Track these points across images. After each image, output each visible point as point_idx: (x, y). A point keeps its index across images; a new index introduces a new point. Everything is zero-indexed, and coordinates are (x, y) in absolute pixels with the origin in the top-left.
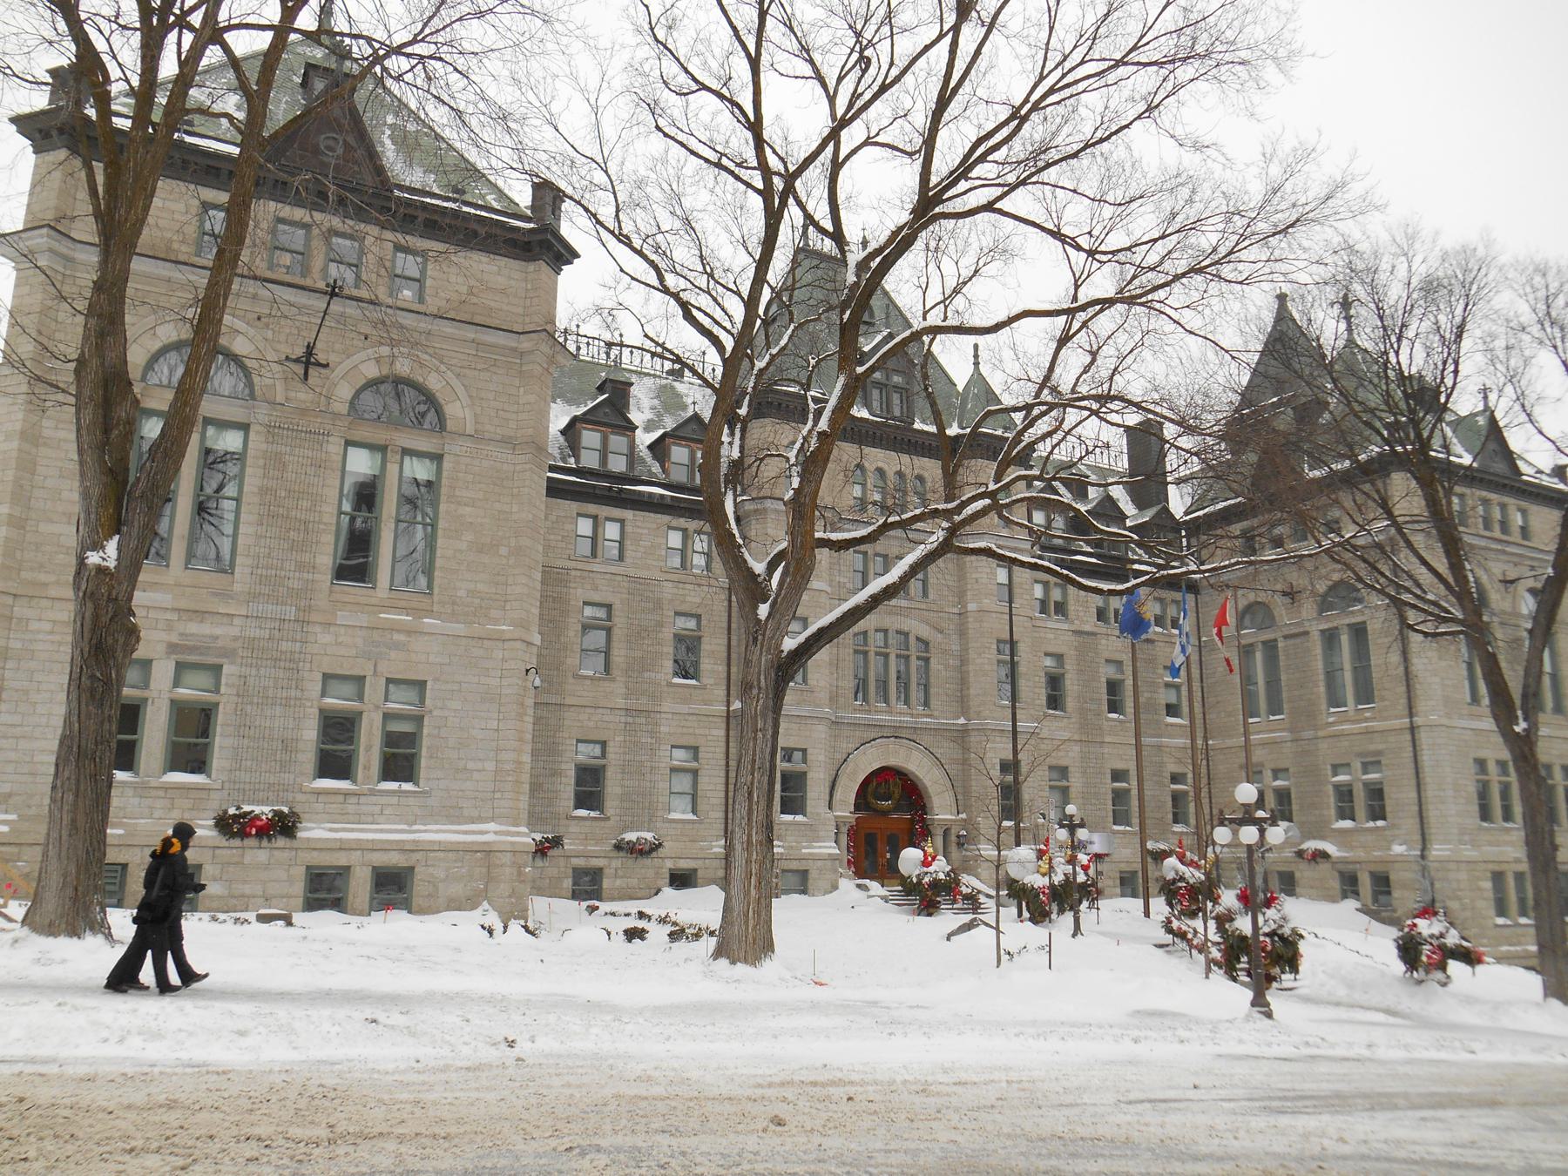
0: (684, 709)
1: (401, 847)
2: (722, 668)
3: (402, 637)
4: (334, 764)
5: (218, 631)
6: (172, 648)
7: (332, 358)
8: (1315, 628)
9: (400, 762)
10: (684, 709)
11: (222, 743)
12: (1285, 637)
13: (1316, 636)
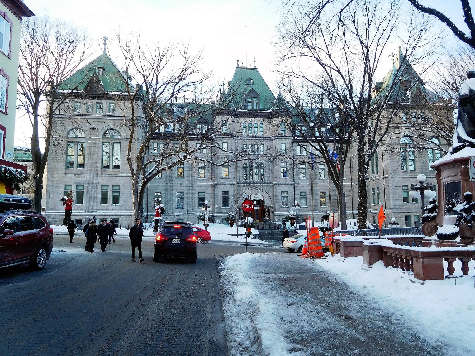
0: (201, 184)
1: (116, 215)
6: (75, 183)
7: (98, 128)
9: (116, 200)
10: (201, 184)
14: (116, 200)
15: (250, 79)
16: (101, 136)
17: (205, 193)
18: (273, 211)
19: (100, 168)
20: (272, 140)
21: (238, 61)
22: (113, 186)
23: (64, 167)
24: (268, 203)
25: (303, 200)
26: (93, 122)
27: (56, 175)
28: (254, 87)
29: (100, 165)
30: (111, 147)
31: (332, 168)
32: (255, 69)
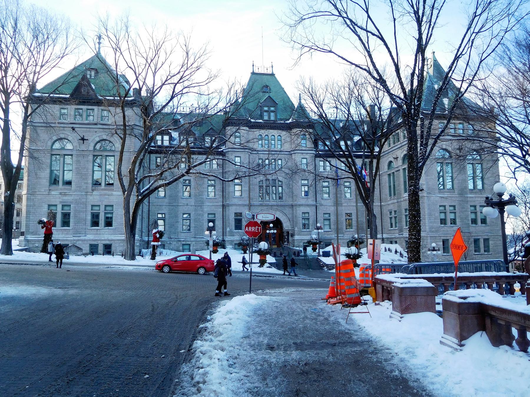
2: (221, 193)
3: (107, 196)
4: (95, 223)
5: (69, 198)
6: (61, 202)
8: (401, 168)
9: (109, 223)
10: (211, 204)
11: (72, 221)
12: (396, 171)
13: (401, 171)
14: (109, 223)
15: (267, 86)
16: (91, 148)
17: (214, 214)
18: (293, 235)
19: (90, 186)
20: (291, 154)
21: (253, 66)
22: (106, 206)
23: (48, 184)
24: (286, 226)
25: (327, 222)
26: (81, 131)
27: (37, 193)
28: (271, 95)
29: (90, 181)
30: (104, 160)
31: (360, 185)
32: (273, 75)
